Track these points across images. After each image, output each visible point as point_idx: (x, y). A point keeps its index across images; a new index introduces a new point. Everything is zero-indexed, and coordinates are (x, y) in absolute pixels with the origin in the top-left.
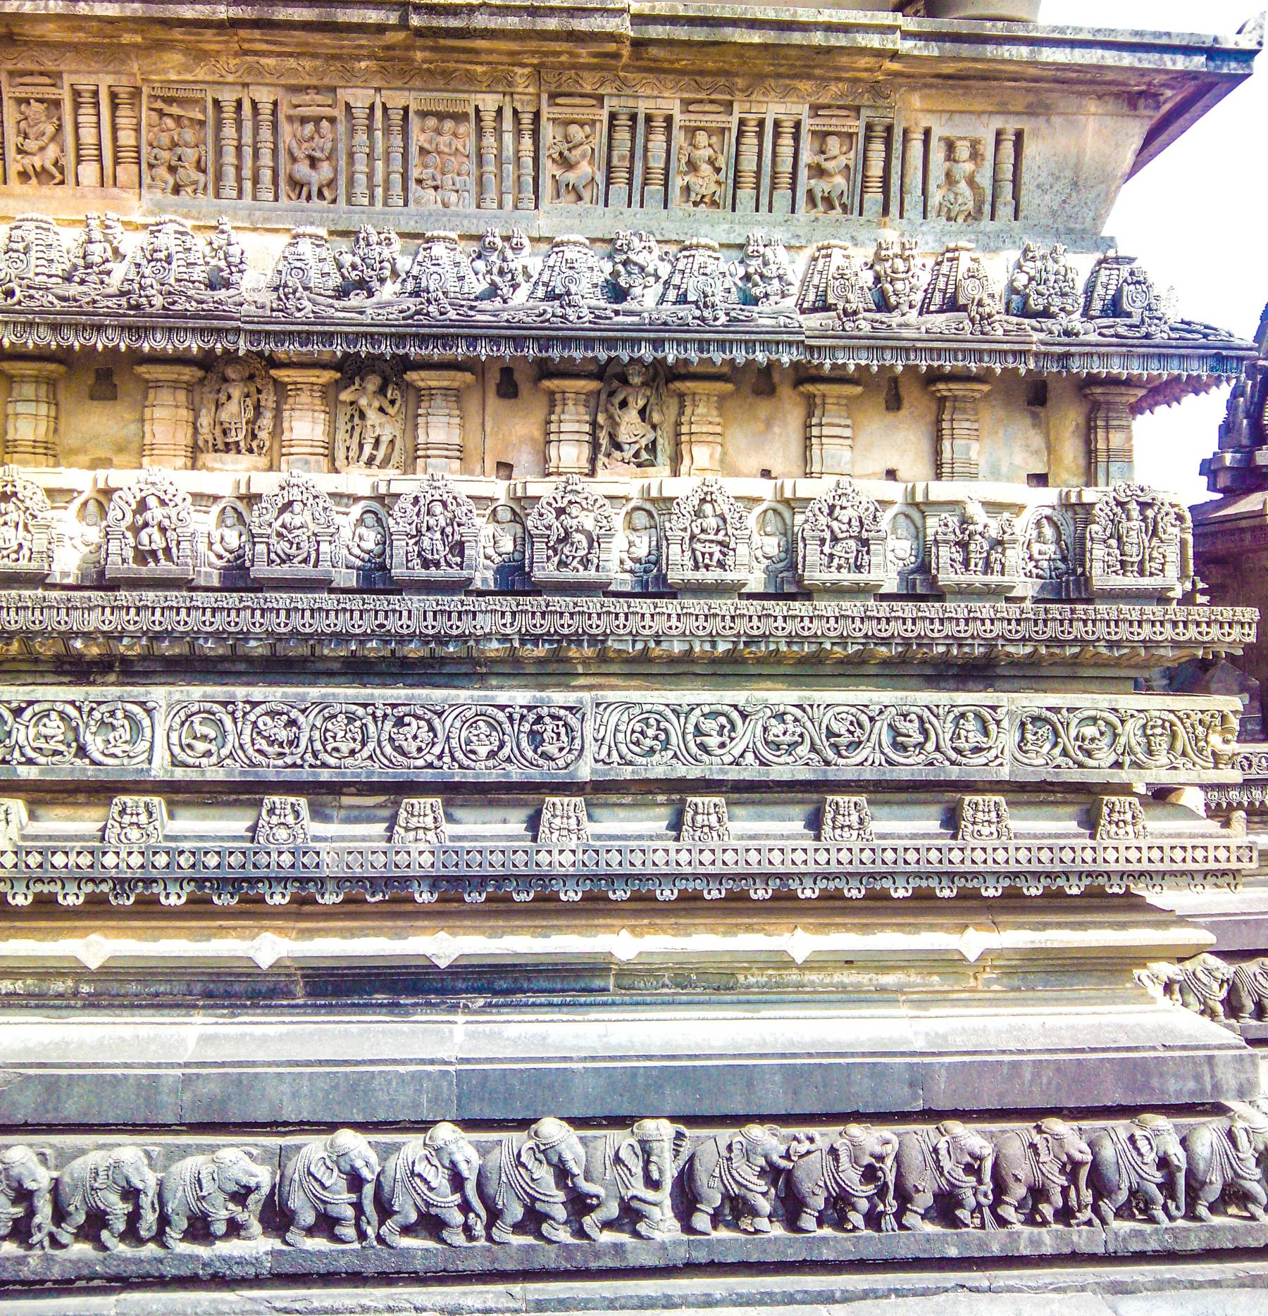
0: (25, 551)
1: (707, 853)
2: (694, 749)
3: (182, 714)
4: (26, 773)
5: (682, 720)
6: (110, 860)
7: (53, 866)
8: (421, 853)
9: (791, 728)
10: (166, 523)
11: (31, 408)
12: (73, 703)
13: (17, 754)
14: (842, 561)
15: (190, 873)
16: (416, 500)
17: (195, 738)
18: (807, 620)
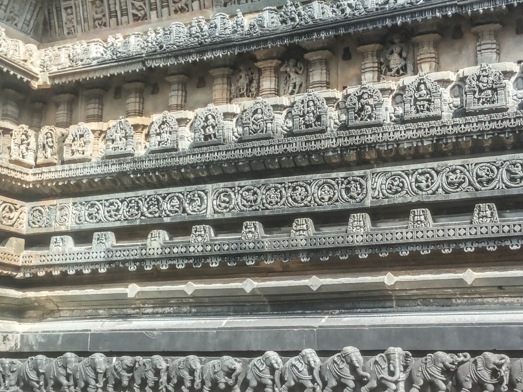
0: (169, 141)
1: (420, 233)
2: (415, 189)
3: (217, 193)
4: (167, 220)
5: (410, 177)
6: (192, 249)
7: (174, 253)
8: (301, 240)
9: (459, 175)
10: (214, 124)
11: (176, 93)
12: (181, 193)
13: (164, 213)
14: (484, 100)
15: (218, 253)
16: (303, 102)
17: (222, 202)
18: (463, 126)
